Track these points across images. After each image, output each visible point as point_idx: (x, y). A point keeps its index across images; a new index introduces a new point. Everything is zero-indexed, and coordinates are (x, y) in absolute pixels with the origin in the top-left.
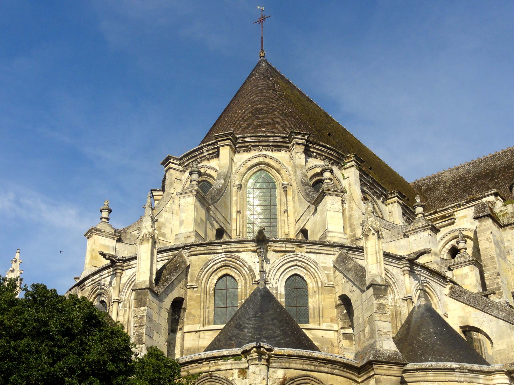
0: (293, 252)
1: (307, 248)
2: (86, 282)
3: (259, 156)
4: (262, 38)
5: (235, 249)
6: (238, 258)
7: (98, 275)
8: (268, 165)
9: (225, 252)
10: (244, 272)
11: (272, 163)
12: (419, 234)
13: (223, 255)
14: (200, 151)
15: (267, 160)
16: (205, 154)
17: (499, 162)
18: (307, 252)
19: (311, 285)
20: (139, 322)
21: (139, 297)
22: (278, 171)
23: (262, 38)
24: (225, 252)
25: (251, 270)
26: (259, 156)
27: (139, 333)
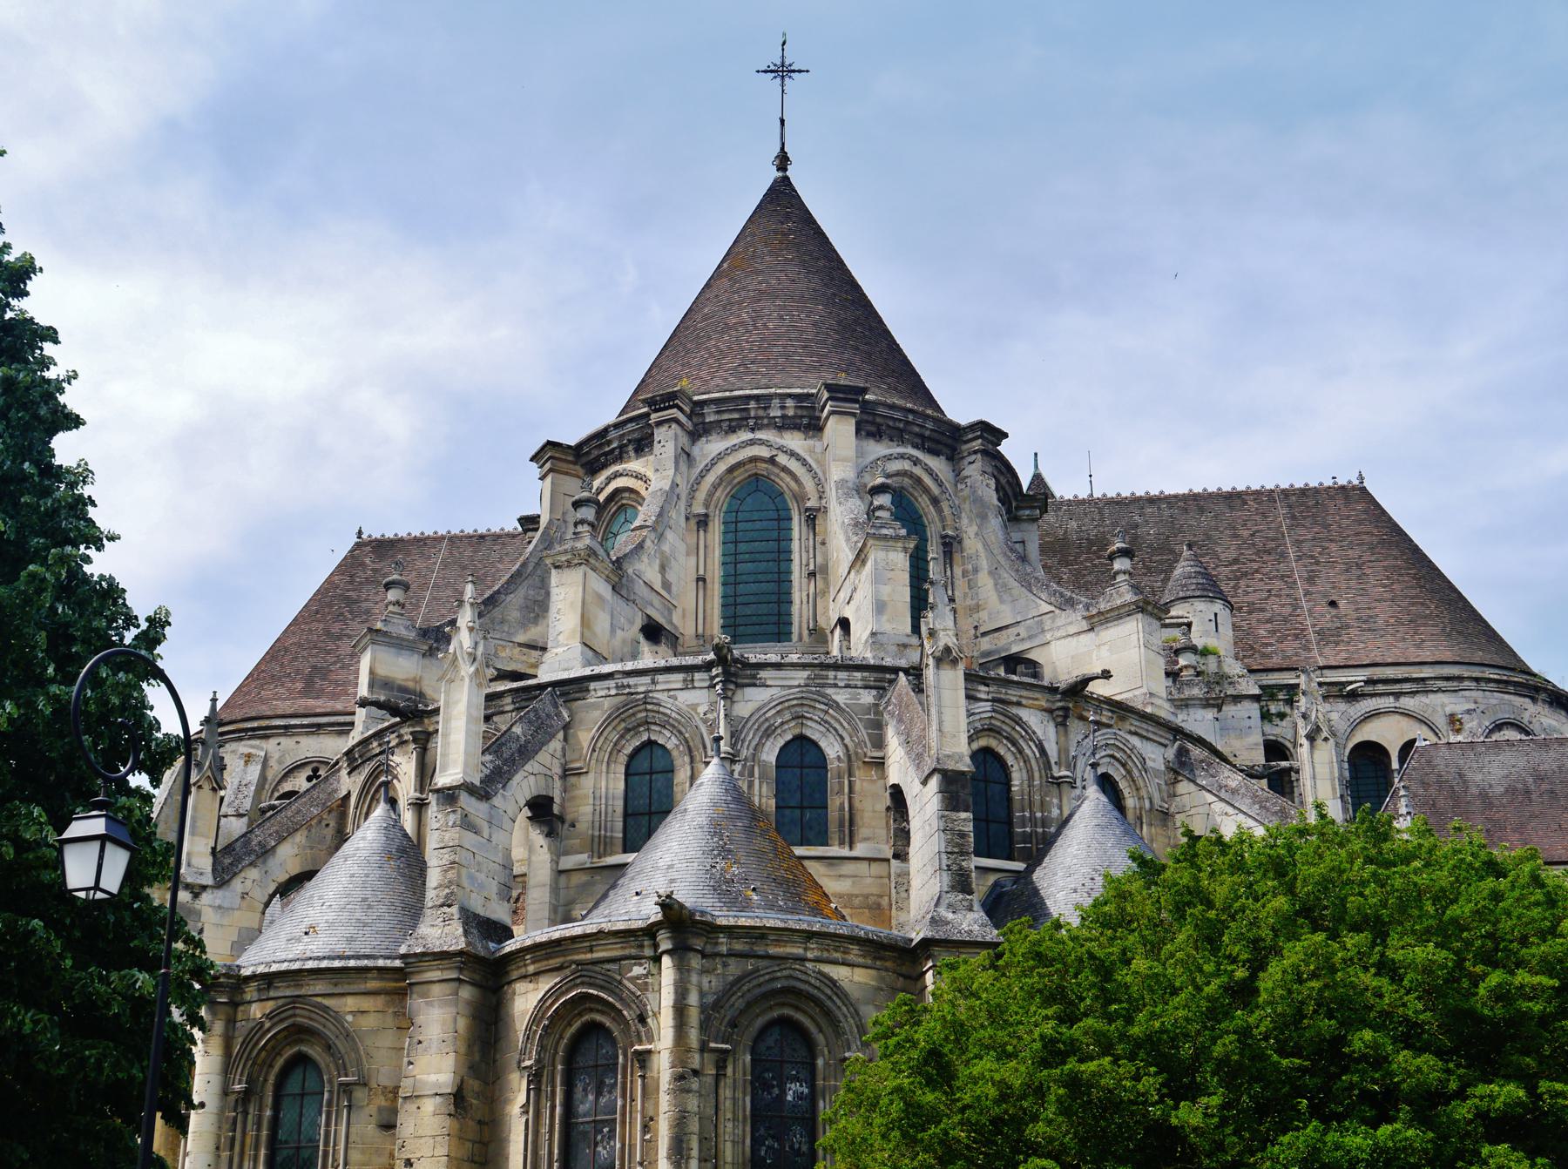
0: (1109, 726)
2: (592, 685)
3: (902, 456)
4: (782, 122)
5: (1014, 699)
6: (1018, 721)
7: (647, 679)
9: (994, 700)
10: (1028, 751)
12: (1192, 711)
13: (987, 706)
15: (918, 471)
17: (1074, 524)
18: (1130, 732)
20: (958, 845)
21: (953, 788)
22: (935, 501)
23: (782, 122)
24: (994, 700)
26: (902, 456)
27: (961, 868)
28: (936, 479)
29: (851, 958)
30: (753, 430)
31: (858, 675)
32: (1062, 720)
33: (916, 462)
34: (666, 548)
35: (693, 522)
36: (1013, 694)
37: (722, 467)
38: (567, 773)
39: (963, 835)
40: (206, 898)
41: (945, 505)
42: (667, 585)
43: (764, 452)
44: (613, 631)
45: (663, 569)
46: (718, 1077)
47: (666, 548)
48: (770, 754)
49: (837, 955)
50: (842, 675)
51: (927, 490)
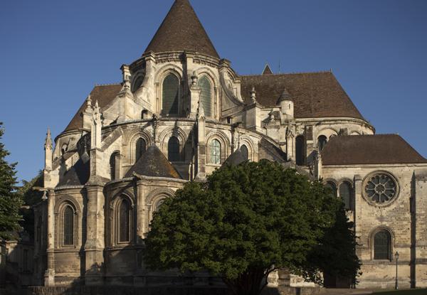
1: (251, 133)
6: (223, 133)
8: (209, 74)
11: (211, 74)
15: (209, 72)
19: (249, 151)
22: (213, 79)
28: (213, 73)
32: (232, 131)
33: (208, 69)
34: (148, 91)
36: (222, 126)
37: (162, 71)
38: (123, 145)
39: (203, 160)
40: (51, 173)
41: (215, 80)
42: (149, 100)
43: (172, 67)
44: (134, 112)
45: (148, 97)
46: (149, 211)
47: (148, 91)
48: (167, 140)
50: (183, 122)
51: (211, 77)
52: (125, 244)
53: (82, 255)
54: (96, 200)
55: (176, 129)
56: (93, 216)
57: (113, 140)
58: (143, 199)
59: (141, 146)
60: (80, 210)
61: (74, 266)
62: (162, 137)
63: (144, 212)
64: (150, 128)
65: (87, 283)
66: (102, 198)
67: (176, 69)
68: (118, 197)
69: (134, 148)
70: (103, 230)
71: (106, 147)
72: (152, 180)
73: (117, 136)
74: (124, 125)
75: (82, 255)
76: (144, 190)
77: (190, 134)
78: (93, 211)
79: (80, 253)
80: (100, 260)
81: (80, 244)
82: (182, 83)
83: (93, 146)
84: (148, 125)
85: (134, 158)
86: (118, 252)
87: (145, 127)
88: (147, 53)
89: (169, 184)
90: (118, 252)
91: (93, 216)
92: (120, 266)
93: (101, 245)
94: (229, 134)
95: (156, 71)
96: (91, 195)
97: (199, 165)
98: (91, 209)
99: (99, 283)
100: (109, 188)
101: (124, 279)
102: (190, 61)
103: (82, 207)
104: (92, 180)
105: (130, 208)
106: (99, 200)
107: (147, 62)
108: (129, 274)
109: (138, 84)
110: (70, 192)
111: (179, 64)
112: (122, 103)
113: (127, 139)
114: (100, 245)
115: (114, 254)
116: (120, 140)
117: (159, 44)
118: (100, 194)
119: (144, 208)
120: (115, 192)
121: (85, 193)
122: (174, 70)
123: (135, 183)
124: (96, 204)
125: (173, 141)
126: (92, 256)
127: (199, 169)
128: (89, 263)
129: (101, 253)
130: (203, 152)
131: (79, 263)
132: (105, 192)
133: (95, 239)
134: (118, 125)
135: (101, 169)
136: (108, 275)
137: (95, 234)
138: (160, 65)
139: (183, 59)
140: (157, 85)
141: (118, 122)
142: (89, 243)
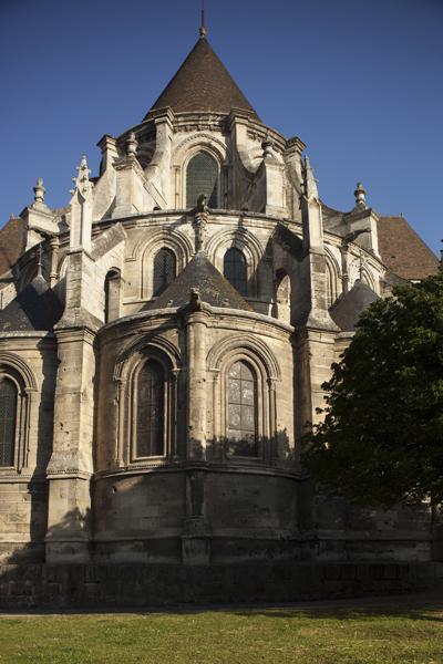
2: (138, 221)
7: (164, 218)
14: (205, 118)
16: (209, 123)
25: (337, 264)
29: (272, 334)
30: (199, 130)
31: (261, 222)
32: (344, 249)
35: (173, 169)
37: (187, 146)
38: (127, 260)
39: (322, 283)
43: (206, 140)
48: (221, 254)
49: (267, 332)
52: (155, 461)
53: (39, 490)
54: (81, 361)
55: (240, 233)
56: (70, 398)
57: (110, 246)
58: (203, 355)
59: (165, 263)
60: (34, 385)
61: (15, 517)
62: (213, 246)
63: (204, 385)
64: (187, 229)
65: (51, 558)
66: (90, 359)
67: (214, 144)
68: (136, 354)
69: (149, 267)
70: (90, 430)
71: (100, 252)
72: (221, 316)
73: (116, 239)
74: (129, 221)
75: (39, 490)
76: (205, 336)
77: (269, 245)
78: (71, 386)
79: (31, 485)
80: (84, 504)
81: (33, 464)
82: (226, 170)
83: (74, 246)
84: (183, 222)
85: (150, 288)
86: (135, 481)
87: (175, 225)
88: (159, 108)
89: (258, 328)
90: (135, 481)
91: (70, 398)
92: (141, 514)
93: (86, 466)
94: (337, 255)
95: (176, 146)
96: (68, 350)
97: (313, 294)
98: (67, 380)
99: (81, 557)
100: (110, 338)
101: (151, 545)
102: (241, 132)
103: (39, 379)
104: (69, 318)
105: (167, 378)
106: (85, 361)
107: (159, 128)
108: (169, 533)
109: (147, 160)
110: (13, 345)
111: (219, 136)
112: (124, 181)
113: (135, 248)
114: (85, 466)
115: (124, 486)
116: (120, 249)
117: (176, 97)
118: (88, 349)
119: (204, 375)
120: (128, 343)
121: (51, 350)
122: (209, 146)
123: (181, 321)
124: (79, 370)
125: (234, 256)
126: (66, 492)
127: (314, 302)
128: (58, 509)
129: (86, 485)
130: (320, 269)
131: (26, 509)
132: (97, 347)
133: (75, 452)
134: (115, 221)
135: (89, 301)
136: (105, 535)
137: (75, 439)
138: (183, 136)
139: (227, 128)
140: (177, 169)
141: (114, 217)
142: (58, 461)
